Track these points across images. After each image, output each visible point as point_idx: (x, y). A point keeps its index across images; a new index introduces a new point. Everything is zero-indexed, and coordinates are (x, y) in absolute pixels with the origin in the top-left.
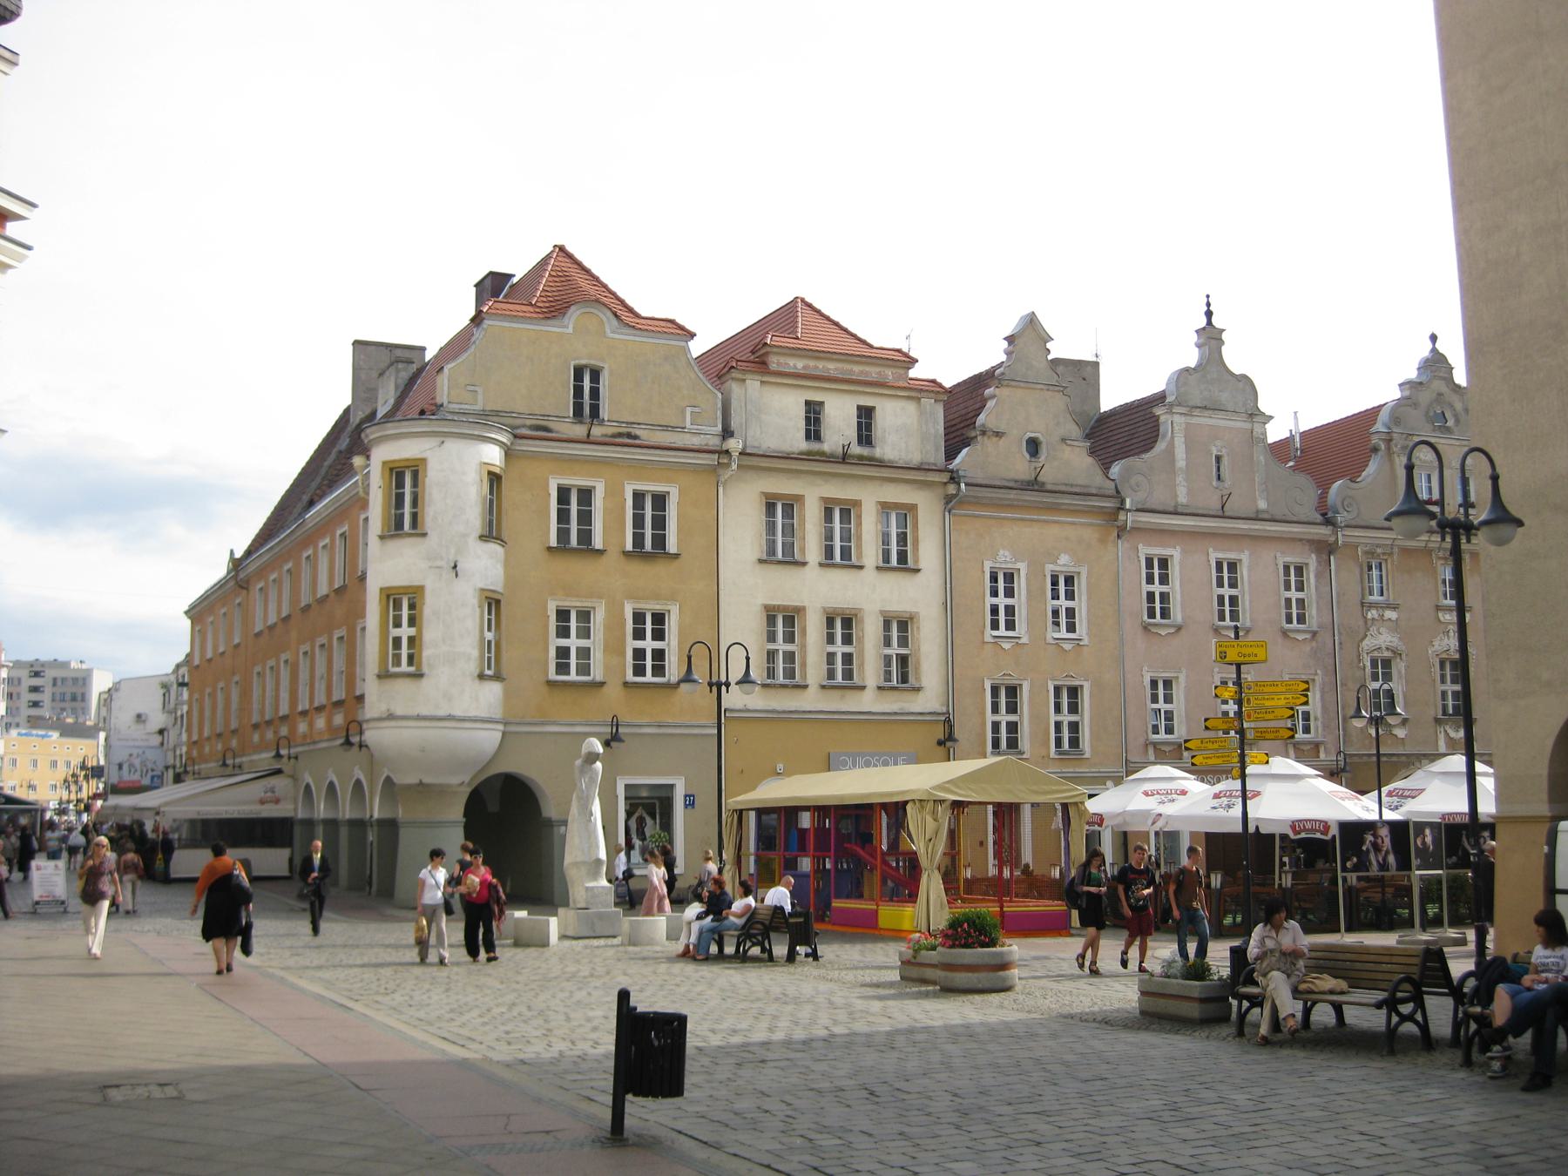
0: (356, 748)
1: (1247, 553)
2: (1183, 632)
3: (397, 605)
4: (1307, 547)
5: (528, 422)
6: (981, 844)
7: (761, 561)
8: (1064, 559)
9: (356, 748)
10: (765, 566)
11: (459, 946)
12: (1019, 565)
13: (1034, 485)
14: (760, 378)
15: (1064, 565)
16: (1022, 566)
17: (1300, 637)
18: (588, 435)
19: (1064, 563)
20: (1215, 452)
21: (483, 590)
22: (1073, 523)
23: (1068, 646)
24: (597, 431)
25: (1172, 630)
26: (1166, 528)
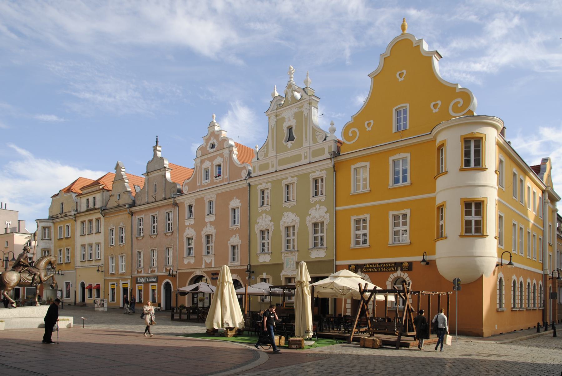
0: (100, 272)
1: (144, 215)
2: (144, 237)
3: (45, 252)
4: (172, 206)
5: (56, 216)
6: (108, 295)
7: (81, 236)
8: (121, 224)
9: (100, 272)
10: (82, 236)
11: (137, 310)
12: (114, 227)
13: (119, 206)
14: (79, 197)
15: (121, 225)
16: (114, 227)
17: (169, 234)
18: (62, 216)
19: (121, 225)
20: (154, 184)
21: (42, 249)
22: (123, 214)
23: (122, 246)
24: (63, 215)
25: (142, 238)
26: (141, 210)
